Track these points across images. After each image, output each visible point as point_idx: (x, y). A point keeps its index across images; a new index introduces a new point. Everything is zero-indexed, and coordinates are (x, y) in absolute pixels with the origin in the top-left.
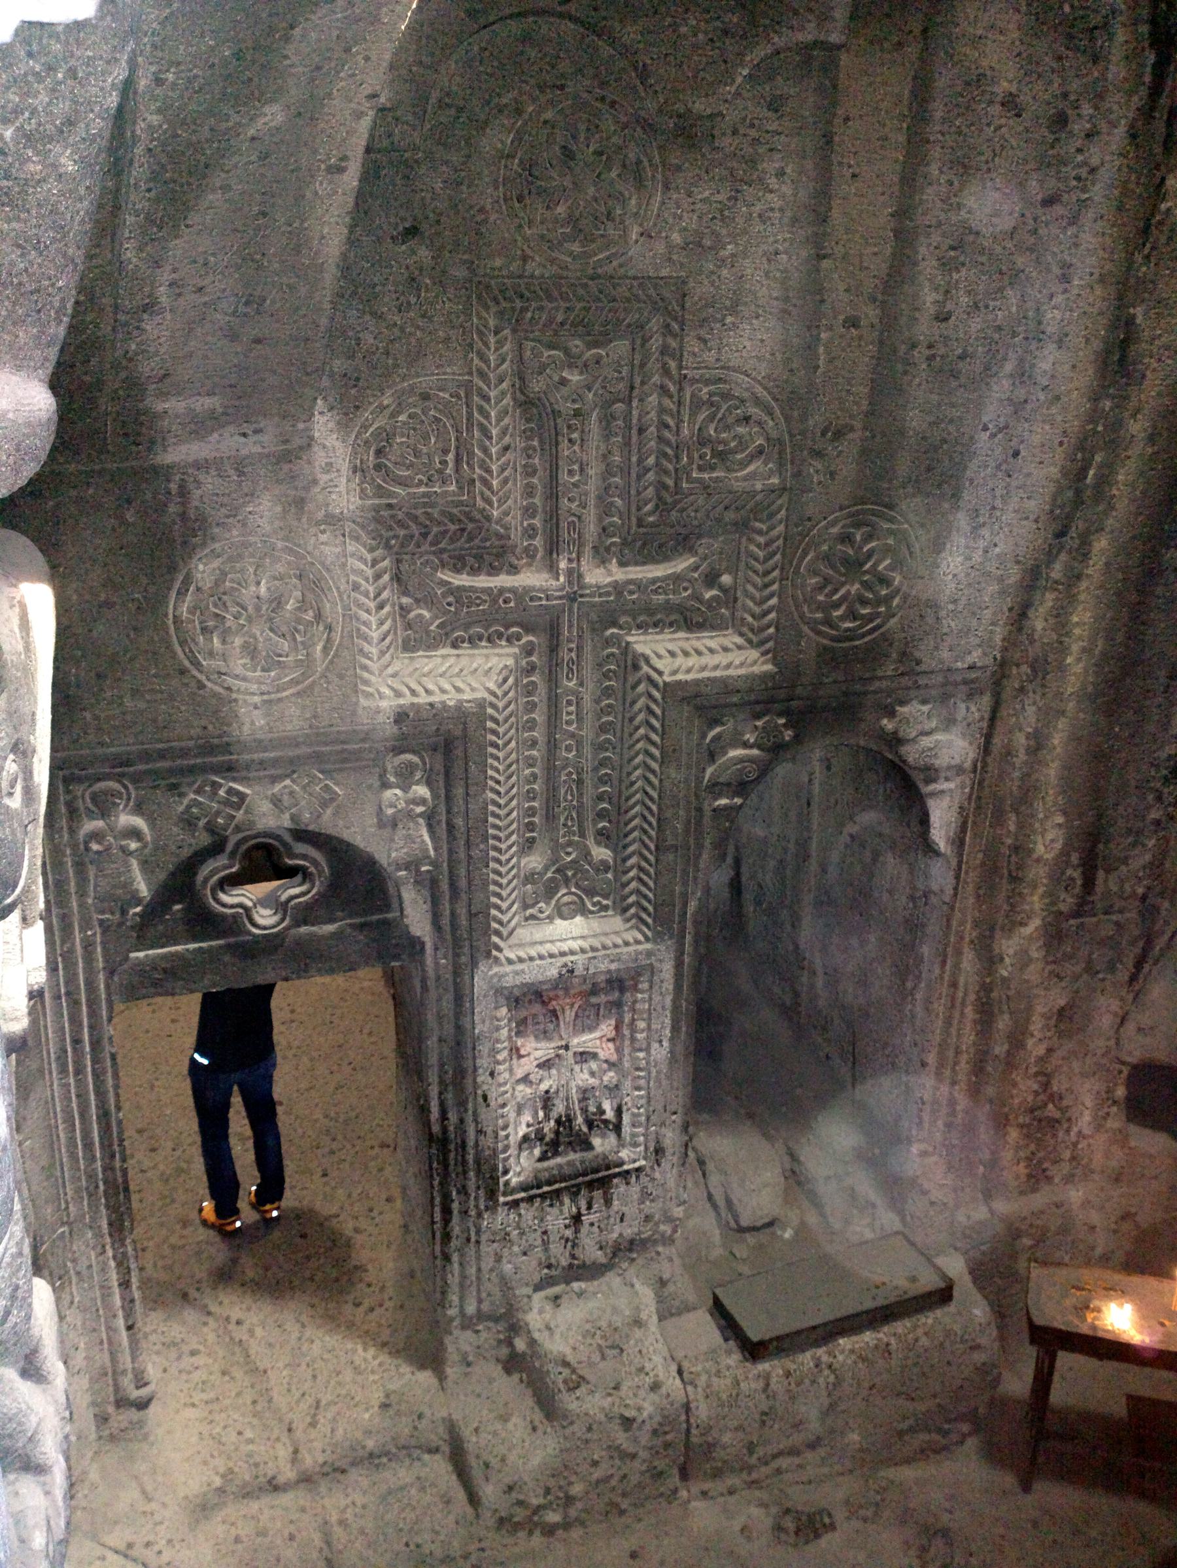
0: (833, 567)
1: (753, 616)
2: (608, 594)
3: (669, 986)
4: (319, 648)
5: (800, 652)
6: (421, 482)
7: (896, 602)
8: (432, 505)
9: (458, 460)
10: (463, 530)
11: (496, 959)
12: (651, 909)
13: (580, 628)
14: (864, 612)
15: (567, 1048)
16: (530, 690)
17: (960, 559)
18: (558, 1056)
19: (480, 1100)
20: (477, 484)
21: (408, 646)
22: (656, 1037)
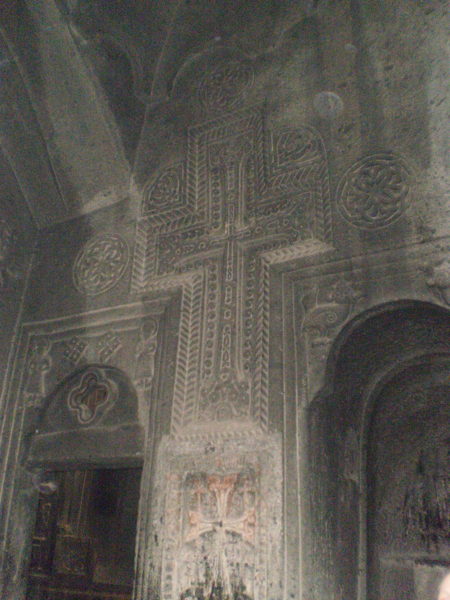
0: (360, 189)
1: (321, 226)
2: (247, 233)
3: (278, 470)
4: (119, 271)
5: (349, 236)
6: (166, 201)
7: (406, 200)
8: (168, 209)
9: (180, 189)
10: (183, 218)
11: (173, 437)
12: (267, 409)
13: (236, 254)
14: (385, 208)
15: (221, 524)
16: (213, 287)
17: (442, 168)
18: (215, 531)
19: (152, 539)
20: (188, 196)
21: (159, 273)
22: (271, 514)
